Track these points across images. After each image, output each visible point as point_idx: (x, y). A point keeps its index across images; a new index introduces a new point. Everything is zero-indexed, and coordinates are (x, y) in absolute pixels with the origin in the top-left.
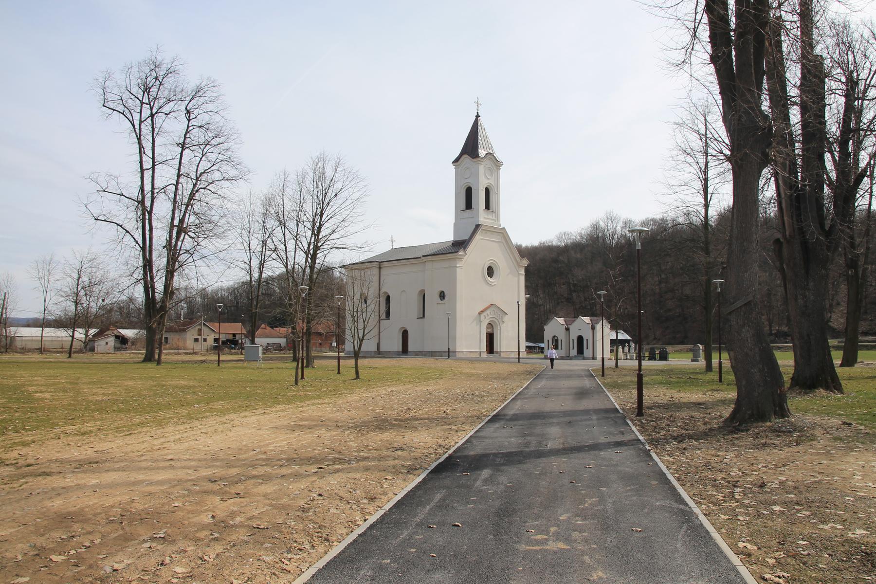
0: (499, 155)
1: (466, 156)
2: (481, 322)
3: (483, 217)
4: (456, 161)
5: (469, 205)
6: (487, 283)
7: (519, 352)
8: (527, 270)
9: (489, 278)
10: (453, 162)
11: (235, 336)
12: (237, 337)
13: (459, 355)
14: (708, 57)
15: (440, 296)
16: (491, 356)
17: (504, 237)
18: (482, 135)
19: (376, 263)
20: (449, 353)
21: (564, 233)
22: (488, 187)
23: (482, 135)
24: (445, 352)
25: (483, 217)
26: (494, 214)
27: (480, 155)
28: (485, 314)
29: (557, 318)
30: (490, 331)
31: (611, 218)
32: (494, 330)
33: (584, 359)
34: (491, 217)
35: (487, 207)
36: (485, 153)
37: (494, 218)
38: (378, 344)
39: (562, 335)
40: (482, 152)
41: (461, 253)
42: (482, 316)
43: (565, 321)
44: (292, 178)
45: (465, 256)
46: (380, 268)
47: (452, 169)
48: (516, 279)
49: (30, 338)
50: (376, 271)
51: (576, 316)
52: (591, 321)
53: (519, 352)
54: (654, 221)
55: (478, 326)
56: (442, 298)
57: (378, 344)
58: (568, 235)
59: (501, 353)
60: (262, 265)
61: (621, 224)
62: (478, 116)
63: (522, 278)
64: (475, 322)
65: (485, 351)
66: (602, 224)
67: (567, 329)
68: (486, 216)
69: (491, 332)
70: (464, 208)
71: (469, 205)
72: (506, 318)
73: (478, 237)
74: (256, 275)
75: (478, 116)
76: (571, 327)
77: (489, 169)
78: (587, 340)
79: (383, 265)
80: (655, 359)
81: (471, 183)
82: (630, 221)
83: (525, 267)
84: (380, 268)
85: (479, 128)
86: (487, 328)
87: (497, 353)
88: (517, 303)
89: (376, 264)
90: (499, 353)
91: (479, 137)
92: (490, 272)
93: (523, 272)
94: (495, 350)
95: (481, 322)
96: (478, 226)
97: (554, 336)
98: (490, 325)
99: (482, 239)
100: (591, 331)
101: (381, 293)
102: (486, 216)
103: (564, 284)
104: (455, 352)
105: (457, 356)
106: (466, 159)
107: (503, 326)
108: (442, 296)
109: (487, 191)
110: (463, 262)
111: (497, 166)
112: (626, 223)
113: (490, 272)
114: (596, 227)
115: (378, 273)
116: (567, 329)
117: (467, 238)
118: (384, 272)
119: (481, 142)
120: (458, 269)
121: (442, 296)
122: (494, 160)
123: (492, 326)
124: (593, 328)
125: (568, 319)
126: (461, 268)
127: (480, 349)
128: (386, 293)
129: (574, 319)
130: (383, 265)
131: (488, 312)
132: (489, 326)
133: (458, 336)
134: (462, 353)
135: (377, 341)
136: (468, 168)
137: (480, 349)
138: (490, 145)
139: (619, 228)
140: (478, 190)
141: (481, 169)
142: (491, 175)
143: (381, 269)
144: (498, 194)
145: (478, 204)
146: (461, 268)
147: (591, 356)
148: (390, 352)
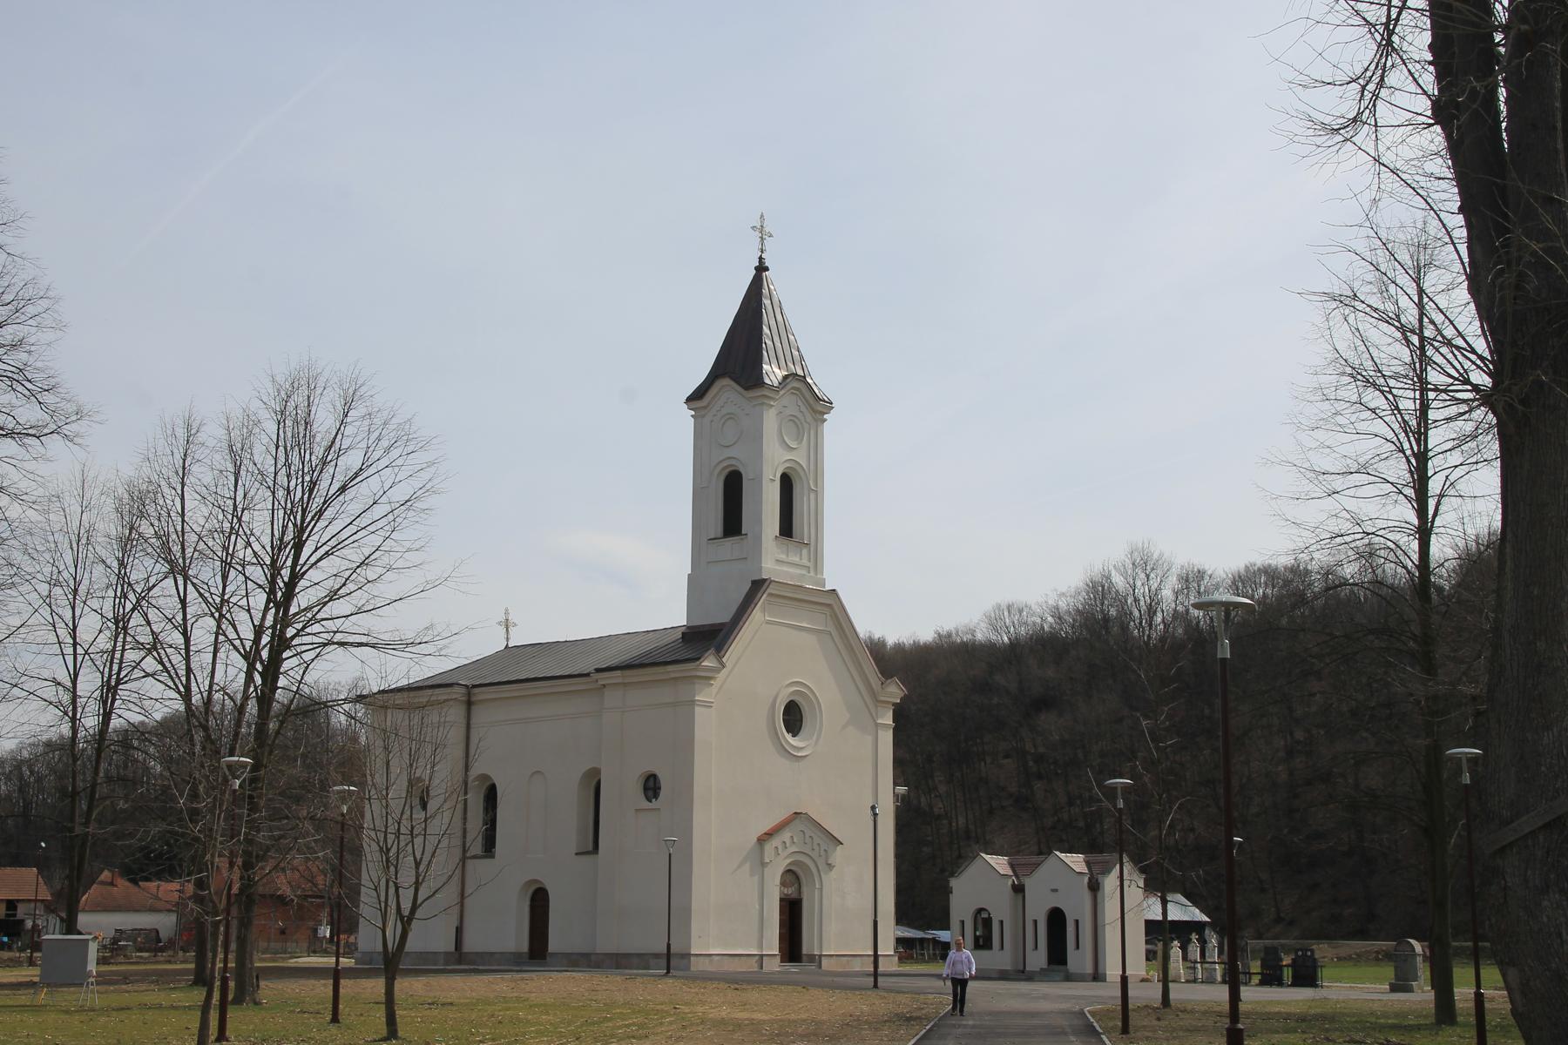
0: (822, 380)
1: (725, 382)
2: (763, 864)
3: (774, 560)
4: (696, 397)
5: (732, 523)
6: (785, 752)
7: (876, 956)
8: (900, 713)
9: (789, 737)
10: (689, 400)
11: (15, 908)
12: (21, 911)
13: (697, 966)
14: (1424, 105)
15: (646, 789)
16: (793, 968)
17: (835, 617)
18: (773, 323)
19: (456, 689)
20: (671, 961)
21: (1009, 607)
23: (773, 323)
24: (657, 956)
25: (774, 560)
26: (805, 552)
27: (767, 381)
28: (775, 842)
29: (987, 857)
30: (790, 891)
31: (1144, 564)
32: (805, 889)
33: (1069, 978)
34: (796, 559)
35: (787, 529)
36: (780, 374)
37: (805, 562)
38: (459, 931)
39: (1001, 909)
40: (773, 372)
41: (709, 662)
42: (769, 847)
43: (1012, 866)
44: (212, 434)
45: (718, 671)
46: (469, 704)
47: (686, 417)
48: (869, 739)
50: (455, 714)
51: (1044, 851)
52: (1088, 864)
53: (876, 956)
54: (1270, 573)
55: (756, 878)
56: (650, 793)
57: (459, 931)
58: (1021, 611)
59: (825, 962)
60: (110, 691)
61: (1172, 582)
62: (761, 268)
63: (887, 738)
64: (747, 866)
66: (1119, 581)
67: (1019, 889)
68: (783, 557)
69: (795, 896)
70: (720, 530)
71: (732, 523)
72: (838, 855)
73: (757, 616)
74: (90, 722)
75: (761, 268)
76: (1029, 883)
77: (793, 419)
78: (1077, 922)
79: (480, 695)
80: (1280, 983)
81: (740, 457)
82: (1201, 574)
83: (894, 704)
84: (469, 704)
85: (766, 302)
86: (783, 884)
87: (812, 958)
88: (869, 811)
89: (458, 693)
90: (816, 959)
91: (766, 330)
92: (794, 717)
93: (888, 719)
94: (805, 951)
95: (763, 864)
96: (758, 585)
97: (980, 911)
98: (792, 876)
99: (768, 622)
100: (1087, 896)
101: (470, 779)
102: (783, 557)
103: (1007, 756)
104: (687, 956)
105: (692, 969)
106: (727, 391)
107: (830, 880)
108: (651, 786)
109: (787, 483)
110: (714, 690)
111: (815, 411)
112: (1192, 579)
113: (794, 717)
114: (1100, 590)
115: (463, 721)
116: (1019, 889)
117: (725, 617)
118: (481, 716)
119: (769, 343)
120: (697, 709)
121: (651, 786)
122: (808, 395)
123: (798, 878)
124: (1094, 887)
125: (1021, 859)
126: (708, 705)
127: (761, 946)
128: (484, 777)
129: (1035, 859)
130: (480, 695)
131: (786, 835)
132: (789, 877)
133: (695, 906)
134: (707, 960)
135: (456, 923)
136: (731, 417)
137: (761, 946)
138: (795, 353)
139: (1167, 593)
140: (758, 480)
141: (770, 420)
142: (799, 438)
143: (473, 707)
144: (817, 492)
145: (759, 521)
146: (708, 705)
147: (1089, 969)
148: (492, 954)
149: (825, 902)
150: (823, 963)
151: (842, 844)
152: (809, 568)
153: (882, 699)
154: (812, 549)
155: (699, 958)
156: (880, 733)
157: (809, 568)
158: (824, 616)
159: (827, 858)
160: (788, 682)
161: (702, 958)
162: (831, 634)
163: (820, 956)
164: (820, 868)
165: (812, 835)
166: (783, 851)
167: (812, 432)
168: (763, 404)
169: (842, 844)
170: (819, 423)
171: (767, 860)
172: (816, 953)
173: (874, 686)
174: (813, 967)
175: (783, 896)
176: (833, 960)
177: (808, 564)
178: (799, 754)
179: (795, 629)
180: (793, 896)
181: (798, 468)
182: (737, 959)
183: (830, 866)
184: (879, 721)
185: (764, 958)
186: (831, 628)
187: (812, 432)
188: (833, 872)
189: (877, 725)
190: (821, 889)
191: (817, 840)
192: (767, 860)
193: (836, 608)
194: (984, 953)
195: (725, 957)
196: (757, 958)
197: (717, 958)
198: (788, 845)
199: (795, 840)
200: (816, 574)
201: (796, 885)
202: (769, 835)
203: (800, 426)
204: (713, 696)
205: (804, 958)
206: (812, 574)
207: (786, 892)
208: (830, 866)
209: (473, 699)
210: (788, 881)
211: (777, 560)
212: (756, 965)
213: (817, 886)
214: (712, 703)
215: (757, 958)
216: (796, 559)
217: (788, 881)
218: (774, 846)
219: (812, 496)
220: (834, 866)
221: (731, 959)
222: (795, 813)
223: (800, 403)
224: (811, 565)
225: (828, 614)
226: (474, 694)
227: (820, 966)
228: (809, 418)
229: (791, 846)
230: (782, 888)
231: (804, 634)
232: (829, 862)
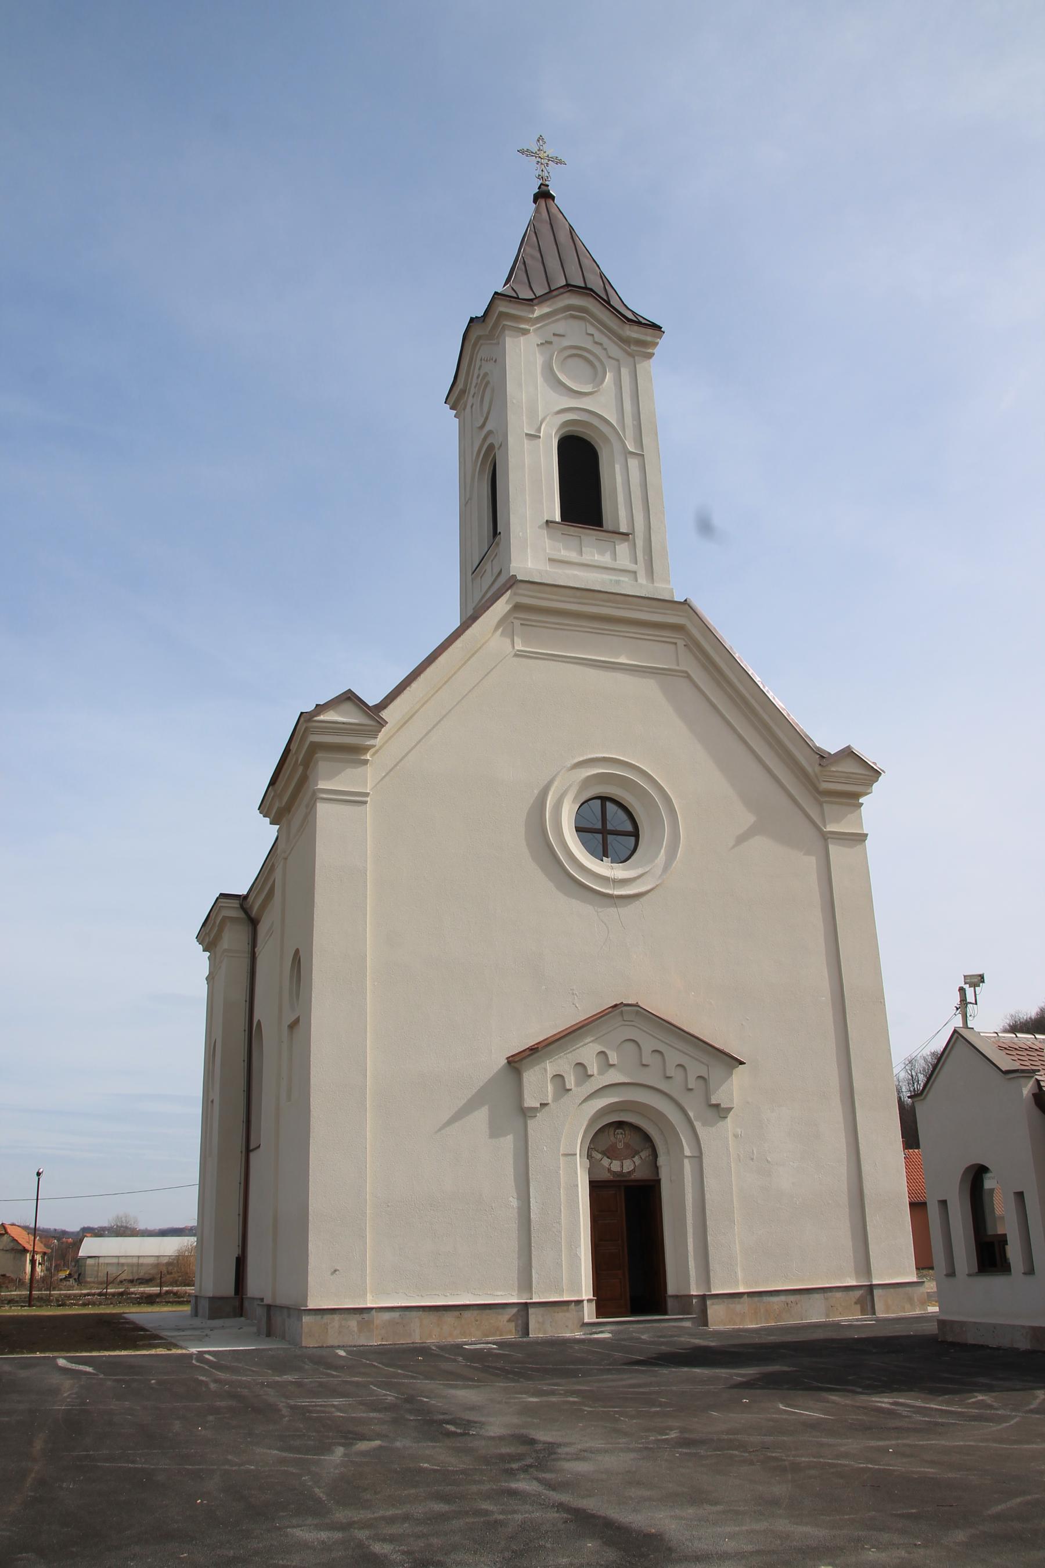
9: (603, 868)
22: (578, 430)
26: (623, 548)
32: (661, 1160)
34: (605, 559)
45: (374, 734)
48: (810, 863)
49: (115, 1260)
55: (508, 1142)
57: (241, 1263)
62: (543, 195)
64: (481, 1116)
65: (591, 1297)
68: (572, 556)
75: (543, 195)
77: (577, 353)
84: (253, 923)
87: (684, 1301)
94: (672, 1289)
102: (572, 556)
111: (626, 341)
120: (323, 809)
123: (647, 1138)
126: (357, 800)
127: (526, 1283)
131: (587, 1051)
132: (621, 1139)
133: (316, 1203)
134: (353, 1323)
135: (236, 1252)
146: (357, 800)
149: (711, 1183)
150: (709, 1312)
151: (742, 1063)
152: (635, 573)
153: (825, 786)
154: (640, 543)
155: (327, 1318)
156: (833, 849)
157: (635, 573)
158: (672, 647)
159: (707, 1098)
160: (581, 759)
161: (336, 1317)
162: (688, 677)
163: (703, 1298)
164: (691, 1114)
165: (661, 1047)
166: (579, 1084)
167: (625, 372)
168: (504, 328)
169: (742, 1063)
170: (636, 358)
171: (530, 1102)
172: (694, 1292)
173: (809, 770)
174: (688, 1324)
175: (605, 1176)
176: (742, 1306)
177: (632, 567)
178: (617, 892)
179: (586, 665)
180: (636, 1176)
181: (596, 422)
182: (449, 1318)
183: (720, 1111)
184: (830, 828)
185: (531, 1311)
186: (690, 665)
187: (625, 372)
188: (729, 1119)
189: (826, 838)
190: (699, 1157)
191: (673, 1057)
192: (530, 1102)
193: (695, 632)
194: (994, 1283)
195: (414, 1314)
196: (514, 1310)
197: (386, 1316)
198: (593, 1068)
199: (613, 1058)
200: (653, 583)
201: (644, 1154)
202: (534, 1052)
203: (597, 364)
204: (369, 786)
205: (670, 1303)
206: (642, 580)
207: (616, 1166)
208: (720, 1111)
209: (253, 914)
210: (620, 1146)
211: (550, 560)
212: (512, 1325)
213: (687, 1152)
214: (367, 795)
215: (514, 1310)
216: (605, 559)
217: (620, 1146)
218: (549, 1076)
219: (633, 464)
220: (729, 1109)
221: (432, 1317)
222: (616, 1006)
223: (591, 330)
224: (641, 568)
225: (681, 643)
226: (251, 907)
227: (706, 1324)
228: (614, 350)
229: (601, 1072)
230: (606, 1162)
231: (620, 676)
232: (714, 1102)
